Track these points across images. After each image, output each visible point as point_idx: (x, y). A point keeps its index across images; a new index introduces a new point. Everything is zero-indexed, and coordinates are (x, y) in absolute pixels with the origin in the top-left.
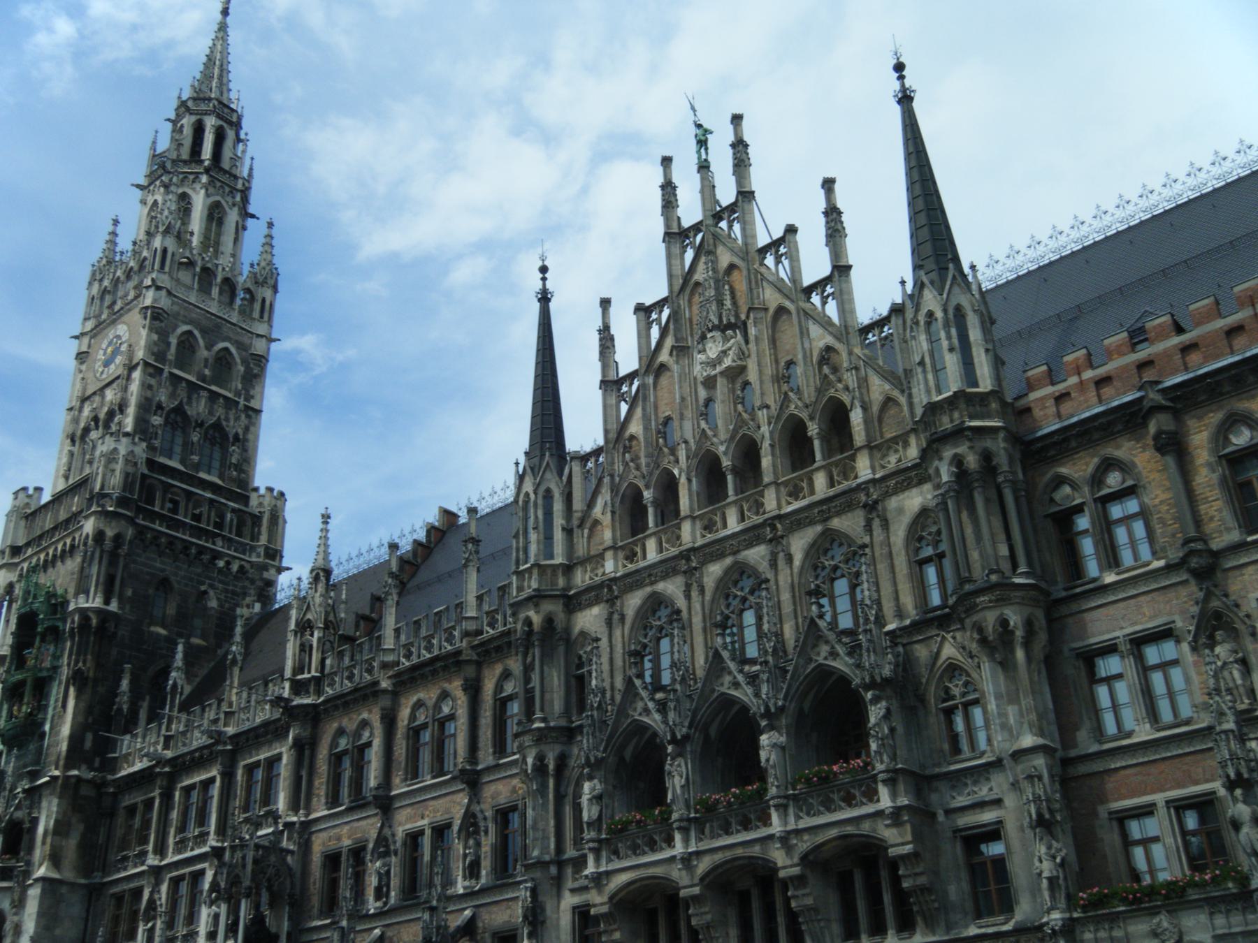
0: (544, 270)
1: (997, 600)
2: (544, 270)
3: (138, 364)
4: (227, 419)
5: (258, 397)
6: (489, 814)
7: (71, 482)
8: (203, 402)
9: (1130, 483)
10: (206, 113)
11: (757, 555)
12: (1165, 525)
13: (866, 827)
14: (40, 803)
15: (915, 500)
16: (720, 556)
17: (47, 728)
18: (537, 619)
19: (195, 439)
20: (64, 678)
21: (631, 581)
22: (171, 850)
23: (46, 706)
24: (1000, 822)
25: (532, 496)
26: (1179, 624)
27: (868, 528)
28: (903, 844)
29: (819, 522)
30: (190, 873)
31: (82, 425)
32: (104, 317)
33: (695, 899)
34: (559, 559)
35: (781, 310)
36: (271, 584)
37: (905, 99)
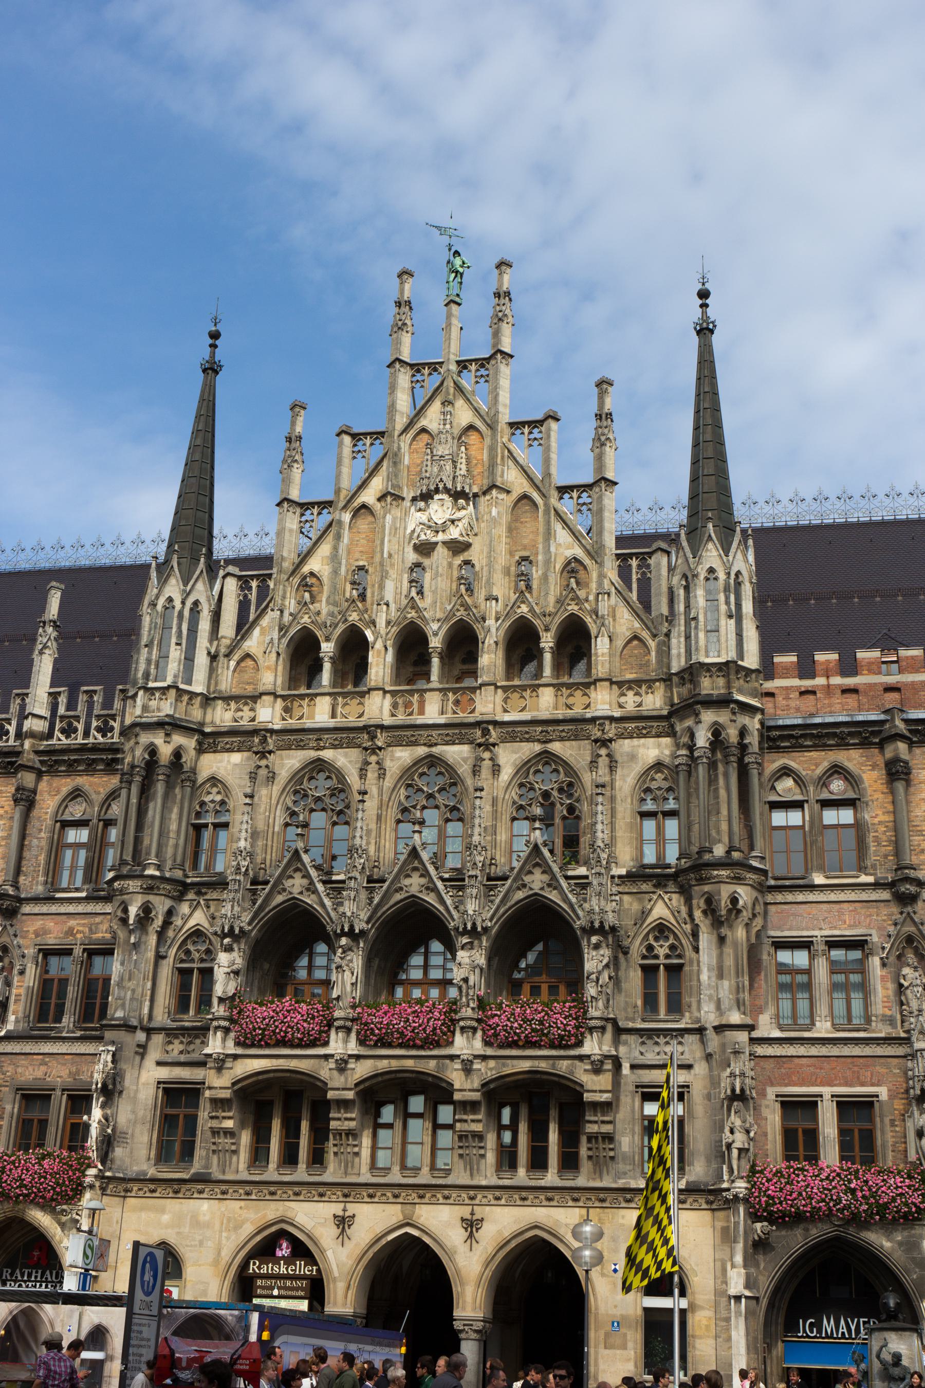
0: (215, 335)
1: (733, 878)
2: (215, 335)
6: (30, 951)
9: (851, 795)
11: (457, 754)
12: (879, 844)
13: (563, 1066)
15: (653, 749)
16: (415, 744)
18: (165, 751)
21: (295, 737)
24: (688, 1087)
25: (178, 604)
26: (875, 939)
27: (593, 764)
28: (601, 1091)
29: (539, 741)
33: (344, 1104)
34: (198, 687)
35: (525, 497)
37: (705, 331)
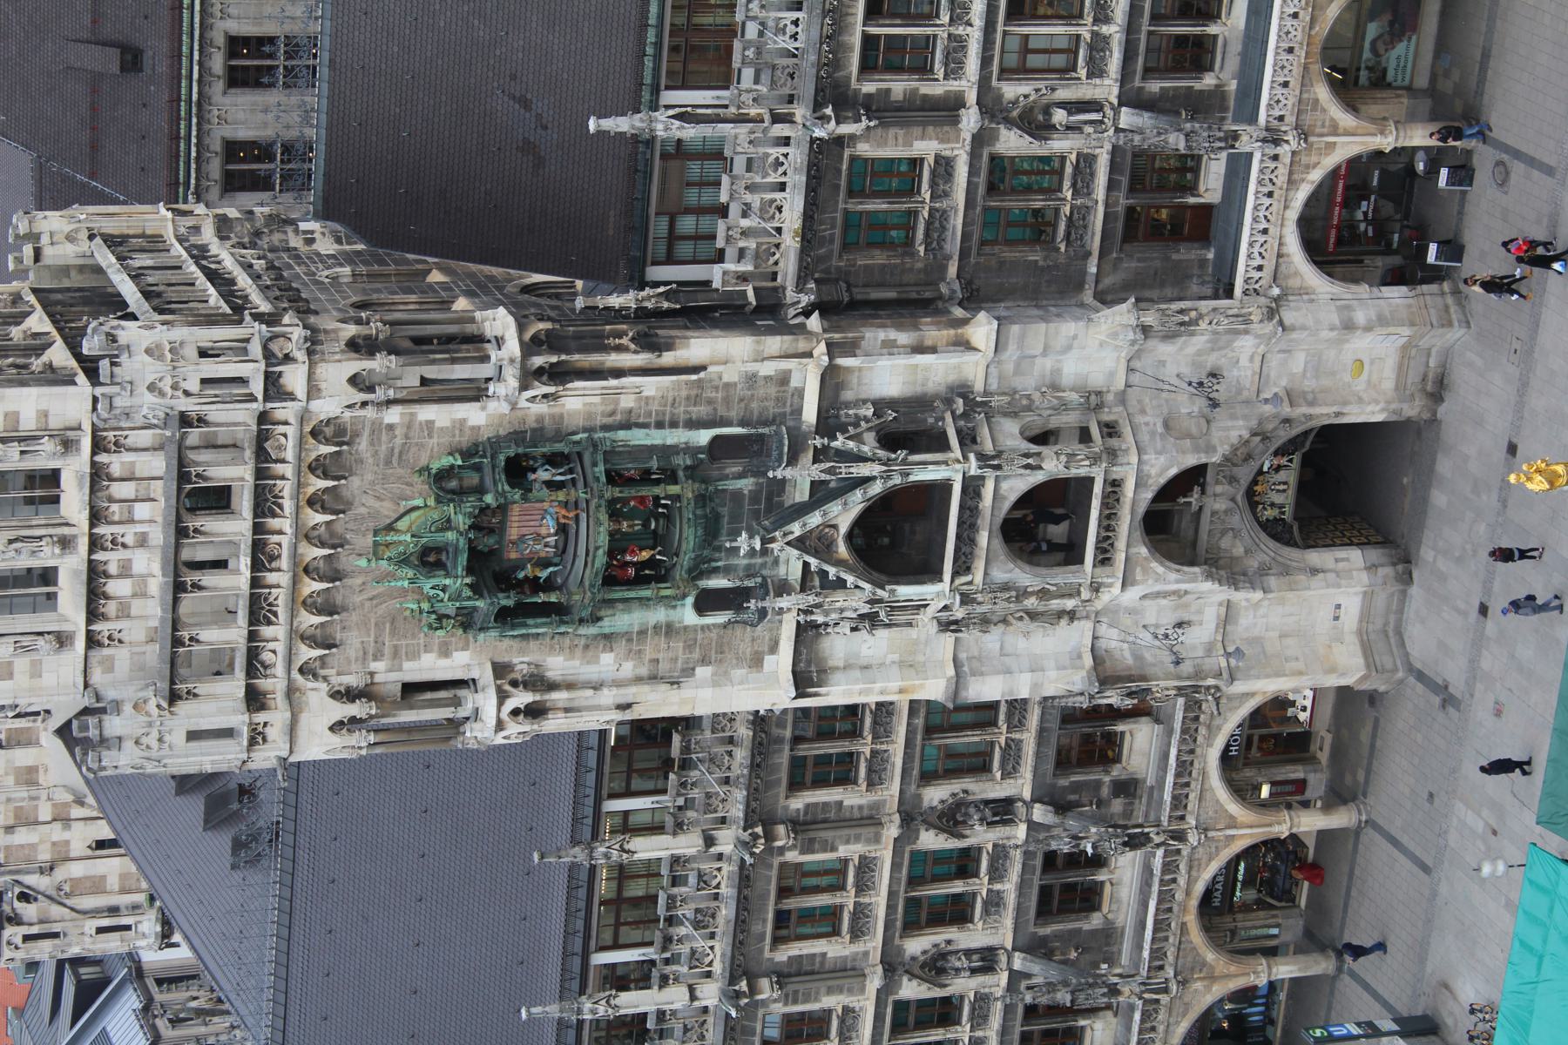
14: (847, 405)
17: (704, 437)
22: (954, 85)
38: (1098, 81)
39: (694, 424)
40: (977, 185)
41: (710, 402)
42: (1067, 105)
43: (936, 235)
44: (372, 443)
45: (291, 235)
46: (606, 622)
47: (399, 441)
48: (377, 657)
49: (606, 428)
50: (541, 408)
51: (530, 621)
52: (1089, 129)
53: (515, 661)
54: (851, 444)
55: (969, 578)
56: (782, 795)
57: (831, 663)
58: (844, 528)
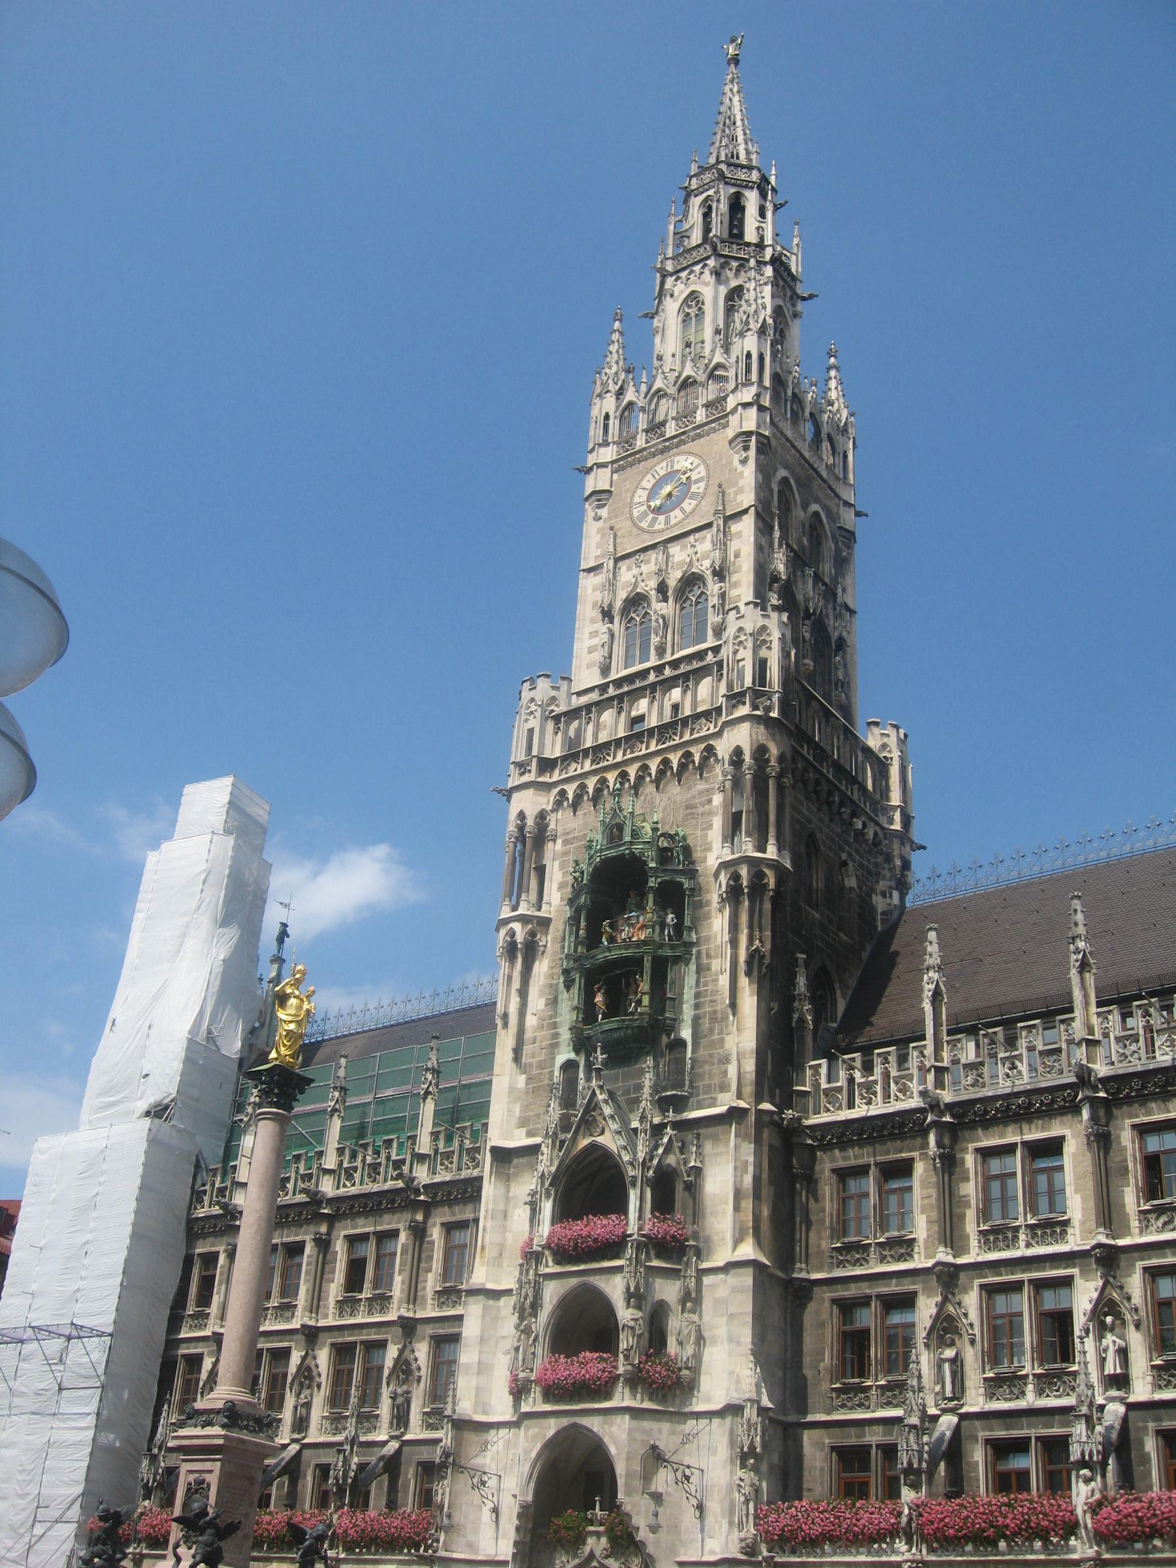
3: (745, 511)
4: (828, 617)
5: (849, 590)
7: (614, 676)
8: (810, 582)
10: (748, 185)
14: (699, 1147)
17: (686, 1033)
19: (807, 635)
20: (720, 965)
22: (974, 1242)
23: (677, 1001)
30: (1030, 1281)
31: (622, 595)
32: (640, 442)
36: (906, 865)
38: (982, 1390)
39: (696, 1021)
40: (889, 1285)
41: (711, 1030)
42: (957, 1362)
43: (848, 1257)
44: (701, 792)
45: (889, 883)
46: (566, 995)
47: (700, 810)
48: (565, 842)
49: (699, 952)
50: (714, 898)
51: (573, 939)
52: (938, 1388)
53: (549, 937)
54: (665, 1140)
55: (551, 1263)
56: (444, 1220)
57: (513, 1185)
58: (599, 1139)
